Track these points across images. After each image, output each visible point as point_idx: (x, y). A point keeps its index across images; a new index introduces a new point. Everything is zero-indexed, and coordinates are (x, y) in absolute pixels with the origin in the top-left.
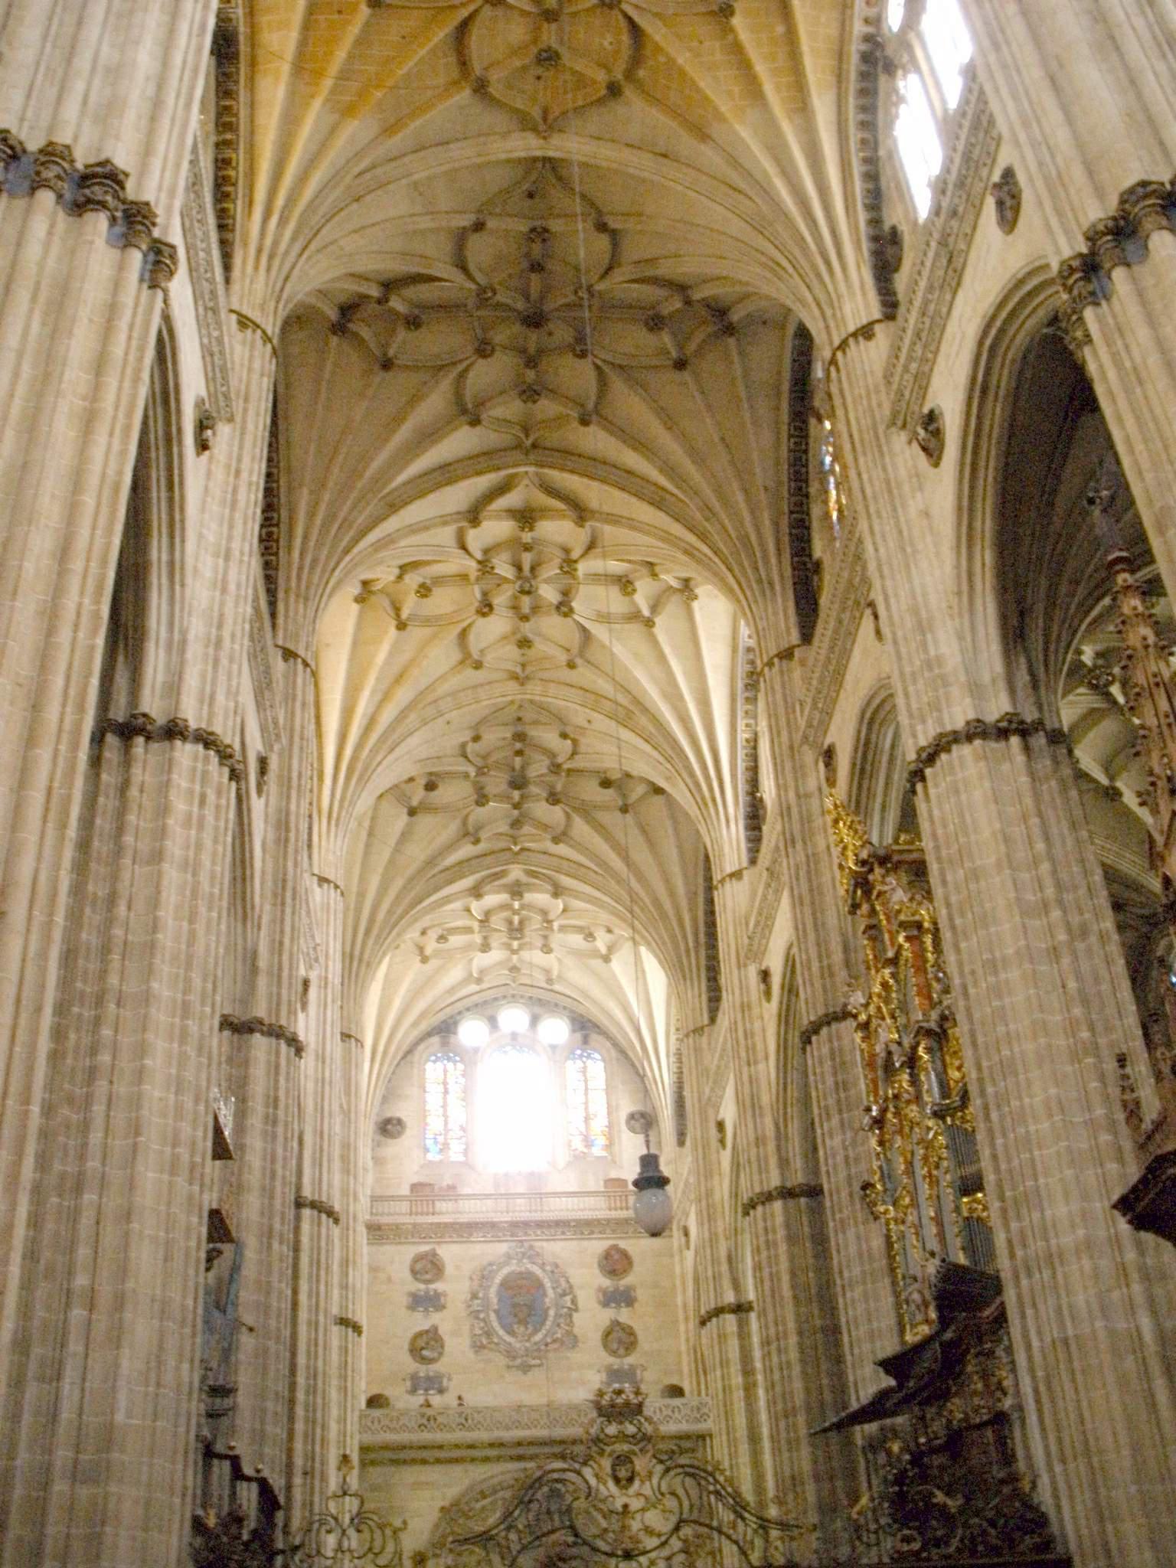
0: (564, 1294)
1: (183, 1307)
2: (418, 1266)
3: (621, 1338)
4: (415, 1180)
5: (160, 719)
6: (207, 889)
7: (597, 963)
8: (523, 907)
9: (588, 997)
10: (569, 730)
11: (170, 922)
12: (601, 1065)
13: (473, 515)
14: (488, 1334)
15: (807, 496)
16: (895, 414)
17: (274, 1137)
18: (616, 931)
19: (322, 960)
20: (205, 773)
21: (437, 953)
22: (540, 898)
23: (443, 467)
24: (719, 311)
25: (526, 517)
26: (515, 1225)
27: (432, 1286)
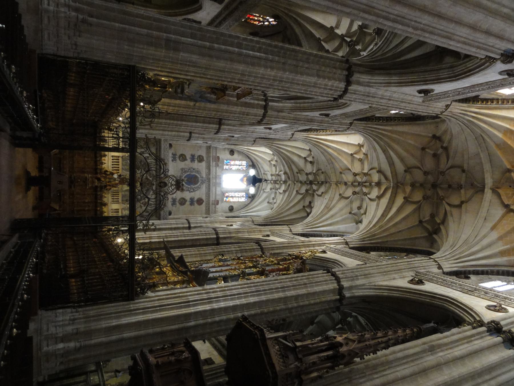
0: (193, 190)
1: (208, 75)
2: (201, 157)
3: (183, 202)
4: (220, 157)
5: (351, 79)
6: (309, 90)
7: (267, 200)
8: (281, 184)
9: (260, 198)
10: (324, 194)
11: (302, 79)
12: (244, 200)
13: (380, 171)
14: (185, 172)
15: (386, 251)
16: (419, 273)
17: (240, 114)
18: (275, 204)
19: (275, 133)
20: (337, 91)
21: (271, 164)
22: (283, 188)
23: (393, 164)
24: (437, 231)
25: (379, 184)
26: (209, 179)
27: (196, 160)
